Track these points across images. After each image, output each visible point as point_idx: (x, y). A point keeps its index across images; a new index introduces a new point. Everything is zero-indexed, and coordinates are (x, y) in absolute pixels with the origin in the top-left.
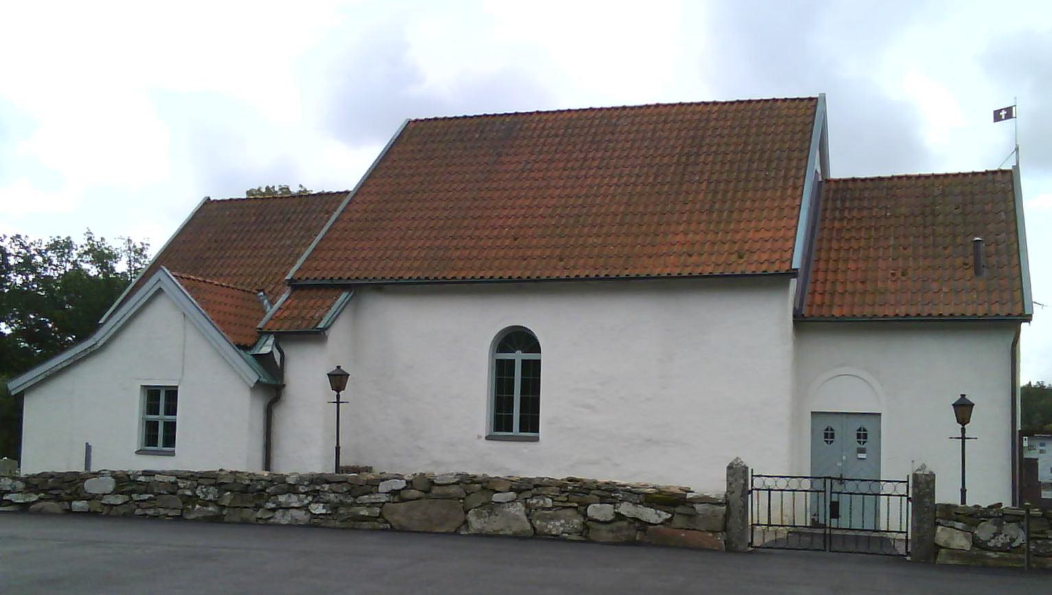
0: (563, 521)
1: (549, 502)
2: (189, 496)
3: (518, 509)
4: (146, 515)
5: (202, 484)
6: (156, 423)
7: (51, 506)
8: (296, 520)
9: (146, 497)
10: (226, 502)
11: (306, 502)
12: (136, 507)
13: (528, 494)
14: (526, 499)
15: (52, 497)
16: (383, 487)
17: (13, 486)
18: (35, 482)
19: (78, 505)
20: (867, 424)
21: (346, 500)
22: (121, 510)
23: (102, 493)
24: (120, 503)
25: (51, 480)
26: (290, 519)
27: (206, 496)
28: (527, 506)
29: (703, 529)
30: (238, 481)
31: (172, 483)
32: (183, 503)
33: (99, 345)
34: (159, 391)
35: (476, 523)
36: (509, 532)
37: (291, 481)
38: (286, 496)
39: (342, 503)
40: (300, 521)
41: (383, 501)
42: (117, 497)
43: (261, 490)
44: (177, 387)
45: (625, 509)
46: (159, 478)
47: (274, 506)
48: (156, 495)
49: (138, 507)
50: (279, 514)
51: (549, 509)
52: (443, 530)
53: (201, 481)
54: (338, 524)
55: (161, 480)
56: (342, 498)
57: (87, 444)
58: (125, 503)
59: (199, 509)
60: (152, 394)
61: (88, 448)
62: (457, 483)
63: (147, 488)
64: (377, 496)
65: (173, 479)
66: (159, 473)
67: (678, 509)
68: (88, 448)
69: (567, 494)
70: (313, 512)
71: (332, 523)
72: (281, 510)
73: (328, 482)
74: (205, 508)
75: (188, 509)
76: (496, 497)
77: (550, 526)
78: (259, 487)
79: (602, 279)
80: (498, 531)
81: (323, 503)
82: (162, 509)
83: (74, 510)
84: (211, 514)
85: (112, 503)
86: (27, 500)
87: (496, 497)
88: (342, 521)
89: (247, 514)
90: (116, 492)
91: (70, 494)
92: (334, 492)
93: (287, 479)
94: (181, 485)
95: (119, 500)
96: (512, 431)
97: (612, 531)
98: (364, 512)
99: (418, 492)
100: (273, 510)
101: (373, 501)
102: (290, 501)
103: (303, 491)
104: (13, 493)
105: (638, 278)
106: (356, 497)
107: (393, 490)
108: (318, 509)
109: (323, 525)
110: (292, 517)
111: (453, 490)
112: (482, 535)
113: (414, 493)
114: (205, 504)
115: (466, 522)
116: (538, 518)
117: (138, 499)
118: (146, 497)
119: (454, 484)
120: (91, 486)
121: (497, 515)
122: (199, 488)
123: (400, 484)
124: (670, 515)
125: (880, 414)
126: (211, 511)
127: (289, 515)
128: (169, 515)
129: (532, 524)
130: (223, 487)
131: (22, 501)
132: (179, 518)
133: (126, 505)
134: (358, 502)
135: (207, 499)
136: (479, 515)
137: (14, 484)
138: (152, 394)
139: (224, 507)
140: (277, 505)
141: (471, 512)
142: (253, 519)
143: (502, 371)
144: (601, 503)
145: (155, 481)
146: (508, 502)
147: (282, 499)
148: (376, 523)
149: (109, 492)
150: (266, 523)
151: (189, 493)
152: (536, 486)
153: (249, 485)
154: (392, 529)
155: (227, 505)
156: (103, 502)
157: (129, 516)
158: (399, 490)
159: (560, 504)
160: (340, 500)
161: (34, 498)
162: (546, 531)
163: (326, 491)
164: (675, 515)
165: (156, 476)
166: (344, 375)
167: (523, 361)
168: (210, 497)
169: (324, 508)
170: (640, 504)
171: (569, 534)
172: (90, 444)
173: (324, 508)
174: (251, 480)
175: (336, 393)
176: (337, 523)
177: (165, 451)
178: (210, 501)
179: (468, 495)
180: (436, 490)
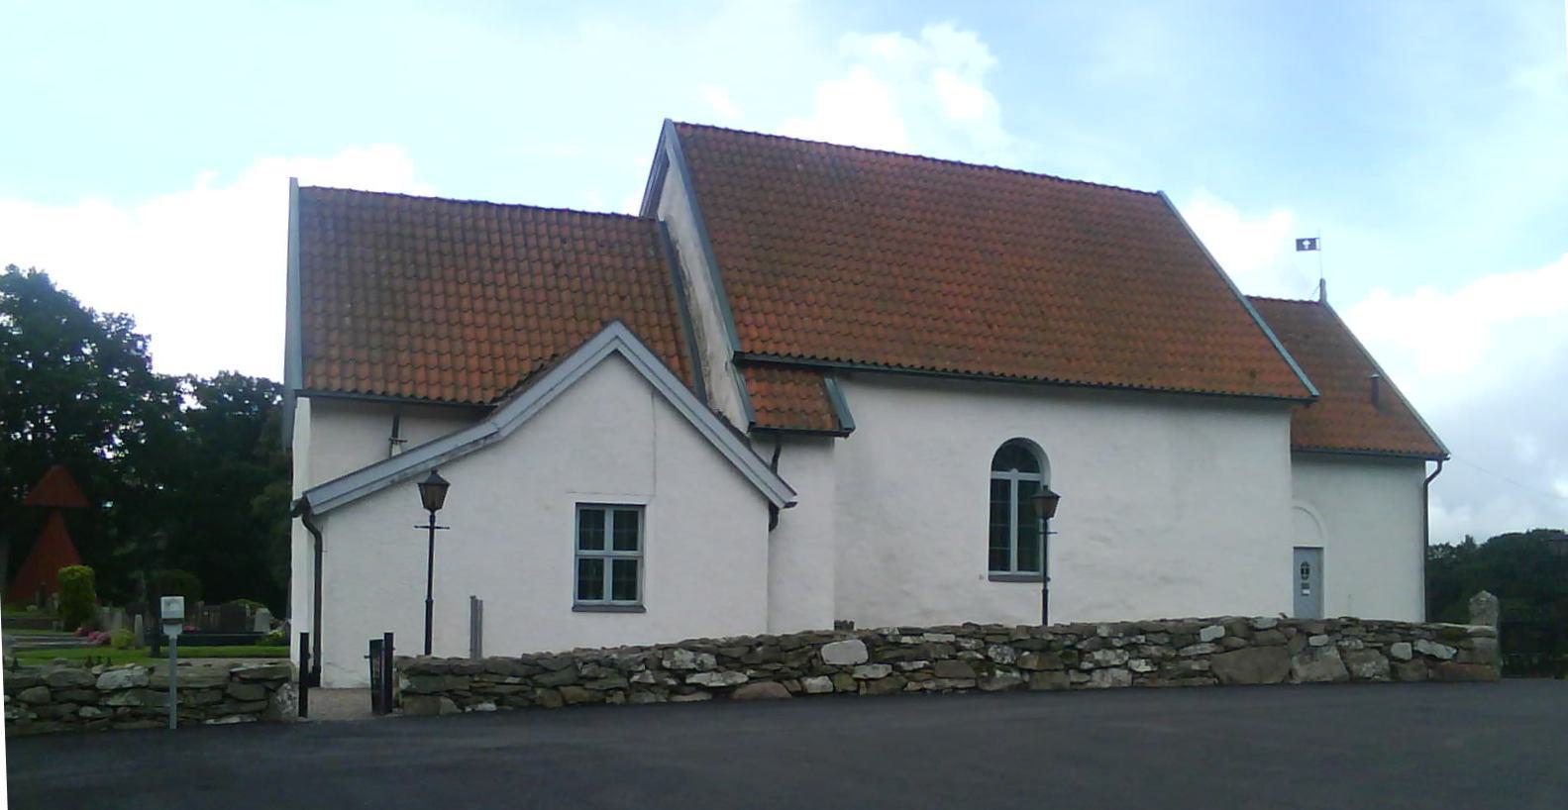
0: (1374, 663)
1: (1360, 644)
2: (980, 660)
3: (1333, 653)
4: (923, 690)
5: (993, 643)
6: (598, 564)
7: (770, 687)
8: (1120, 681)
9: (921, 664)
10: (1033, 664)
11: (1126, 658)
12: (905, 680)
13: (1339, 636)
14: (1337, 641)
15: (768, 674)
16: (1206, 635)
17: (699, 662)
18: (736, 652)
19: (816, 684)
20: (1309, 558)
21: (1169, 653)
22: (886, 686)
23: (853, 663)
24: (882, 676)
25: (760, 649)
26: (1110, 680)
27: (1003, 659)
28: (1341, 650)
29: (1483, 662)
30: (1038, 636)
31: (951, 643)
32: (975, 669)
33: (504, 434)
34: (603, 512)
35: (1302, 672)
36: (1329, 679)
37: (1103, 632)
38: (1101, 652)
39: (1164, 658)
40: (1124, 682)
41: (1208, 652)
42: (874, 668)
43: (1068, 647)
44: (644, 506)
45: (1423, 646)
46: (927, 637)
47: (1091, 665)
48: (931, 662)
49: (910, 679)
50: (1097, 675)
51: (1361, 650)
52: (1271, 682)
53: (989, 638)
54: (1167, 682)
55: (936, 640)
56: (1165, 651)
57: (473, 598)
58: (889, 675)
59: (1001, 677)
60: (590, 517)
61: (476, 606)
62: (1276, 628)
63: (919, 652)
64: (1203, 646)
65: (952, 638)
66: (927, 631)
67: (1462, 644)
68: (476, 606)
69: (1372, 634)
70: (1138, 670)
71: (1161, 682)
72: (1098, 671)
73: (1142, 632)
74: (1009, 674)
75: (983, 677)
76: (1313, 641)
77: (1364, 669)
78: (1068, 643)
79: (1125, 388)
80: (1319, 678)
81: (1143, 658)
82: (947, 680)
83: (810, 691)
84: (1017, 682)
85: (871, 676)
86: (730, 682)
87: (1313, 641)
88: (1172, 679)
89: (1059, 678)
90: (874, 659)
91: (797, 669)
92: (1155, 644)
93: (1099, 631)
94: (967, 646)
95: (881, 671)
96: (1009, 570)
97: (1415, 670)
98: (1196, 667)
99: (1241, 640)
100: (1089, 671)
101: (1200, 652)
102: (1107, 658)
103: (1119, 645)
104: (699, 672)
105: (1162, 390)
106: (1177, 649)
107: (1216, 639)
108: (1142, 666)
109: (1151, 685)
110: (1114, 678)
111: (1276, 635)
112: (1309, 684)
113: (1236, 641)
114: (1006, 668)
115: (1291, 673)
116: (1353, 660)
117: (911, 668)
118: (921, 664)
119: (1272, 628)
120: (832, 653)
121: (1317, 661)
122: (992, 649)
123: (1220, 632)
124: (1455, 651)
125: (1320, 549)
126: (1016, 679)
127: (1109, 676)
128: (959, 686)
129: (1348, 669)
130: (1017, 645)
131: (723, 685)
132: (975, 691)
133: (888, 678)
134: (1183, 655)
135: (1005, 662)
136: (1302, 662)
137: (700, 658)
138: (590, 517)
139: (1030, 671)
140: (1095, 665)
141: (1295, 658)
142: (1067, 685)
143: (999, 490)
144: (1403, 641)
145: (928, 641)
146: (1325, 645)
147: (1098, 656)
148: (1205, 679)
149: (864, 661)
150: (1076, 689)
151: (979, 656)
152: (1345, 626)
153: (1050, 641)
154: (1221, 685)
155: (1034, 668)
156: (855, 676)
157: (899, 694)
158: (1220, 638)
159: (1369, 645)
160: (1163, 654)
161: (741, 678)
162: (1361, 674)
163: (1143, 644)
164: (1461, 651)
165: (925, 634)
166: (1049, 497)
167: (1020, 482)
168: (1008, 660)
169: (1147, 664)
170: (1433, 640)
171: (1381, 676)
172: (478, 598)
173: (1147, 664)
174: (1054, 634)
175: (429, 513)
176: (1167, 682)
177: (583, 606)
178: (1008, 664)
179: (1289, 639)
180: (1259, 636)
